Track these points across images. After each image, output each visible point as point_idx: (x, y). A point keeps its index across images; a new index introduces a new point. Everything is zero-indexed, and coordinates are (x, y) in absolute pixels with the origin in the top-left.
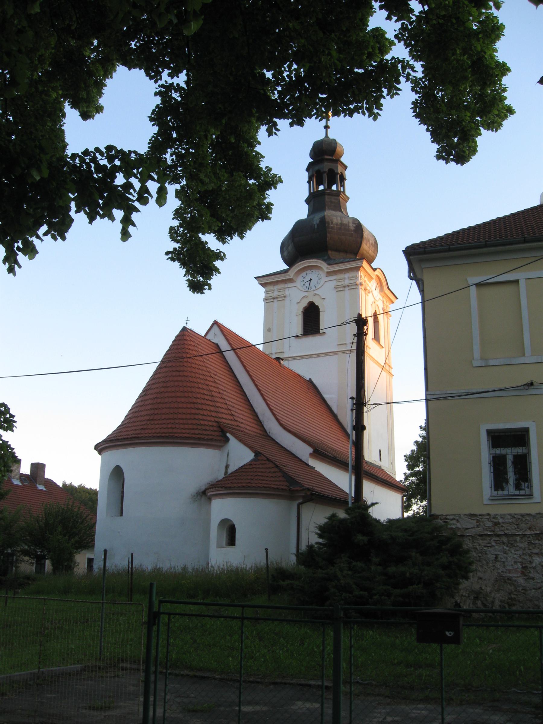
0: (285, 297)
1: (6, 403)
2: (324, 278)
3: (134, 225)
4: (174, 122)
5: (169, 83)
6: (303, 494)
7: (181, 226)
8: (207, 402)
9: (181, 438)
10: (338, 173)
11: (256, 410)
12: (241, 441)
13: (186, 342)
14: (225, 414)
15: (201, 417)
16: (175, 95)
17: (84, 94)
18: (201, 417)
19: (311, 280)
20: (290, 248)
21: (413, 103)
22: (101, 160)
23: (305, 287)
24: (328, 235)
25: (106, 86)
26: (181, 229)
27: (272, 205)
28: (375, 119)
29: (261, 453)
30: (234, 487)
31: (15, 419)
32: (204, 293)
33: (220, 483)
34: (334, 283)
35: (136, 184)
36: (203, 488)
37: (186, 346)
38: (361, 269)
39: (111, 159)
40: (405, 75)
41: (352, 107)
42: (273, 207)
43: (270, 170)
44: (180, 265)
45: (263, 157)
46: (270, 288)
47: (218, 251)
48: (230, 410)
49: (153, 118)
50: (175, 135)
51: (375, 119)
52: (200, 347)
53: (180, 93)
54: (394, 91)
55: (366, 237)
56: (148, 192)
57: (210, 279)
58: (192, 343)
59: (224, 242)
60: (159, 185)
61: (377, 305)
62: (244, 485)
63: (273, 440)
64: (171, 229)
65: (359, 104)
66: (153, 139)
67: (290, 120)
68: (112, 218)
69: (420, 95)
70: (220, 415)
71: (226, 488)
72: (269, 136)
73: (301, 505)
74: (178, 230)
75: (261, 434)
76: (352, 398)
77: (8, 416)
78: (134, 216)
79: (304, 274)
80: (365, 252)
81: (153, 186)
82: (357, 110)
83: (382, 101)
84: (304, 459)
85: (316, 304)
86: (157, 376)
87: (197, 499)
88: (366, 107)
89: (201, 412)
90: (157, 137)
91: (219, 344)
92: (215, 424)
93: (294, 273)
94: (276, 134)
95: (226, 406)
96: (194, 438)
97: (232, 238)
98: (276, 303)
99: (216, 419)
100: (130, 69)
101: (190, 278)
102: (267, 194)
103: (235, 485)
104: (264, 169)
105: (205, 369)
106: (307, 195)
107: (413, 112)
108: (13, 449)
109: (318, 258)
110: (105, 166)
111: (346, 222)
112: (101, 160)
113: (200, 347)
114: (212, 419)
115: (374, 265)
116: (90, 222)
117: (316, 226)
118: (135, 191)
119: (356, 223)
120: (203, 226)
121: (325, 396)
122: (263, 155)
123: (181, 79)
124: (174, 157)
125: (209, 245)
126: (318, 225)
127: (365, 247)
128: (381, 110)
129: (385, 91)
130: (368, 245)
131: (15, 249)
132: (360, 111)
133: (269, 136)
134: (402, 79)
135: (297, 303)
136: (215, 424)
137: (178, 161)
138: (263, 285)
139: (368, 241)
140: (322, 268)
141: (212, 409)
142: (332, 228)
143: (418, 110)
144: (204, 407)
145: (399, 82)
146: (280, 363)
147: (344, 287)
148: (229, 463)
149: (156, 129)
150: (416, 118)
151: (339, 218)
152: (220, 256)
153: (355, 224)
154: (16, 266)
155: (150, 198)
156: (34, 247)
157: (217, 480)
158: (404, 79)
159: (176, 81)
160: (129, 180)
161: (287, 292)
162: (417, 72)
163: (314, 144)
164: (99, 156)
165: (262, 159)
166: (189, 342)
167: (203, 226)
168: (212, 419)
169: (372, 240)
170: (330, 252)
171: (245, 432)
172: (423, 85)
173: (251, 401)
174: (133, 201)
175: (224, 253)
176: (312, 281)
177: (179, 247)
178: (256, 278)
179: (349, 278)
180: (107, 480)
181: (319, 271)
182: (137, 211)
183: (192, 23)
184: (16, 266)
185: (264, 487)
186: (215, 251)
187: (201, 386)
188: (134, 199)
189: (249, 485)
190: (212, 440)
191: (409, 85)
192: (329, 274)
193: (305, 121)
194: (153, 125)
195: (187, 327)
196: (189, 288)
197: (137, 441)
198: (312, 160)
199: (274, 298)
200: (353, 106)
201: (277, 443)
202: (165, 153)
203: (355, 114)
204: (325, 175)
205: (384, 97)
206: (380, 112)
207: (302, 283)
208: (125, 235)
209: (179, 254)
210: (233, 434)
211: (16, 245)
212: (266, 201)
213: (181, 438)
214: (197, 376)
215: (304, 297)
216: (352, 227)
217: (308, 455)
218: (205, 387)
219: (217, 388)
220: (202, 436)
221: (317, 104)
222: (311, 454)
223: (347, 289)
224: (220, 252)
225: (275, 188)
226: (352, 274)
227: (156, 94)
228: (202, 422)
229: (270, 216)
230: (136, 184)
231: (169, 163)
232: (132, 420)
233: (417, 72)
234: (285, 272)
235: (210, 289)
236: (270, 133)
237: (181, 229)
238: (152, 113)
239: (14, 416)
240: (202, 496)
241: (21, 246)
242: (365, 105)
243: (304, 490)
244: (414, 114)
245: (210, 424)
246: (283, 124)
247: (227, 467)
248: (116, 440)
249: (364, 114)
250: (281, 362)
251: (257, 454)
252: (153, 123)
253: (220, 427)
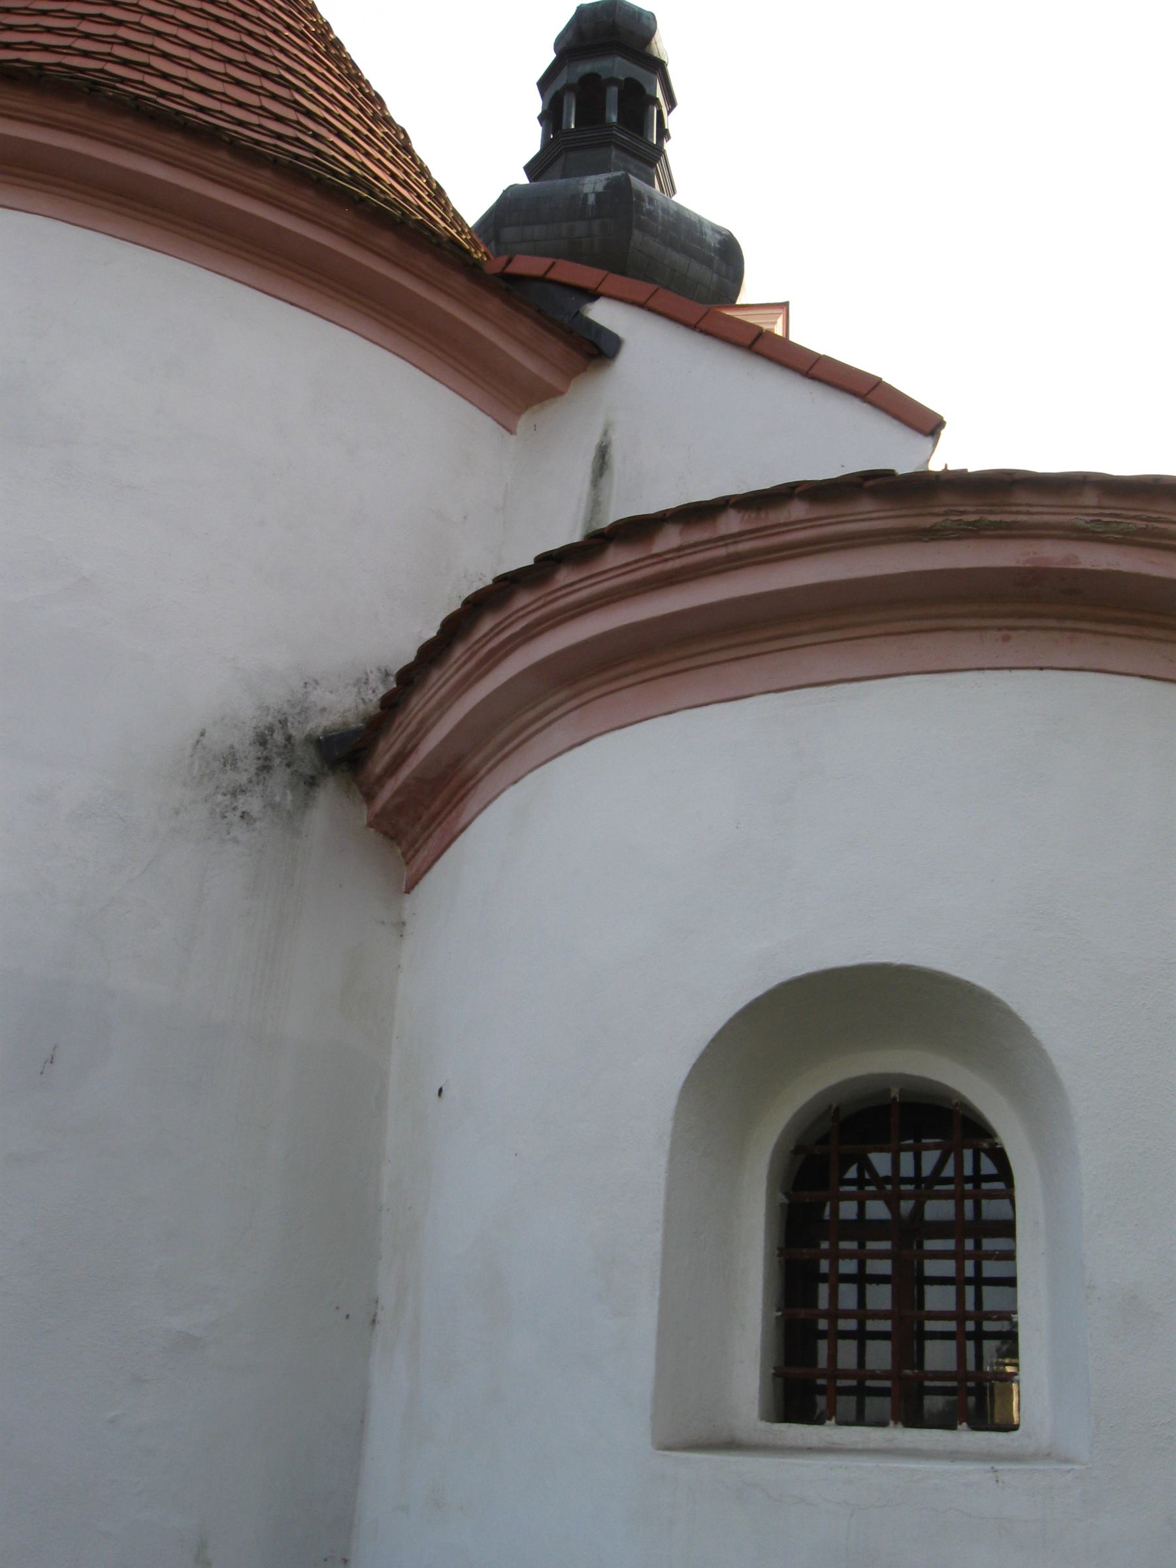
24: (637, 234)
87: (253, 804)
117: (591, 199)
126: (598, 195)
142: (650, 214)
163: (578, 8)
204: (613, 92)
240: (312, 782)
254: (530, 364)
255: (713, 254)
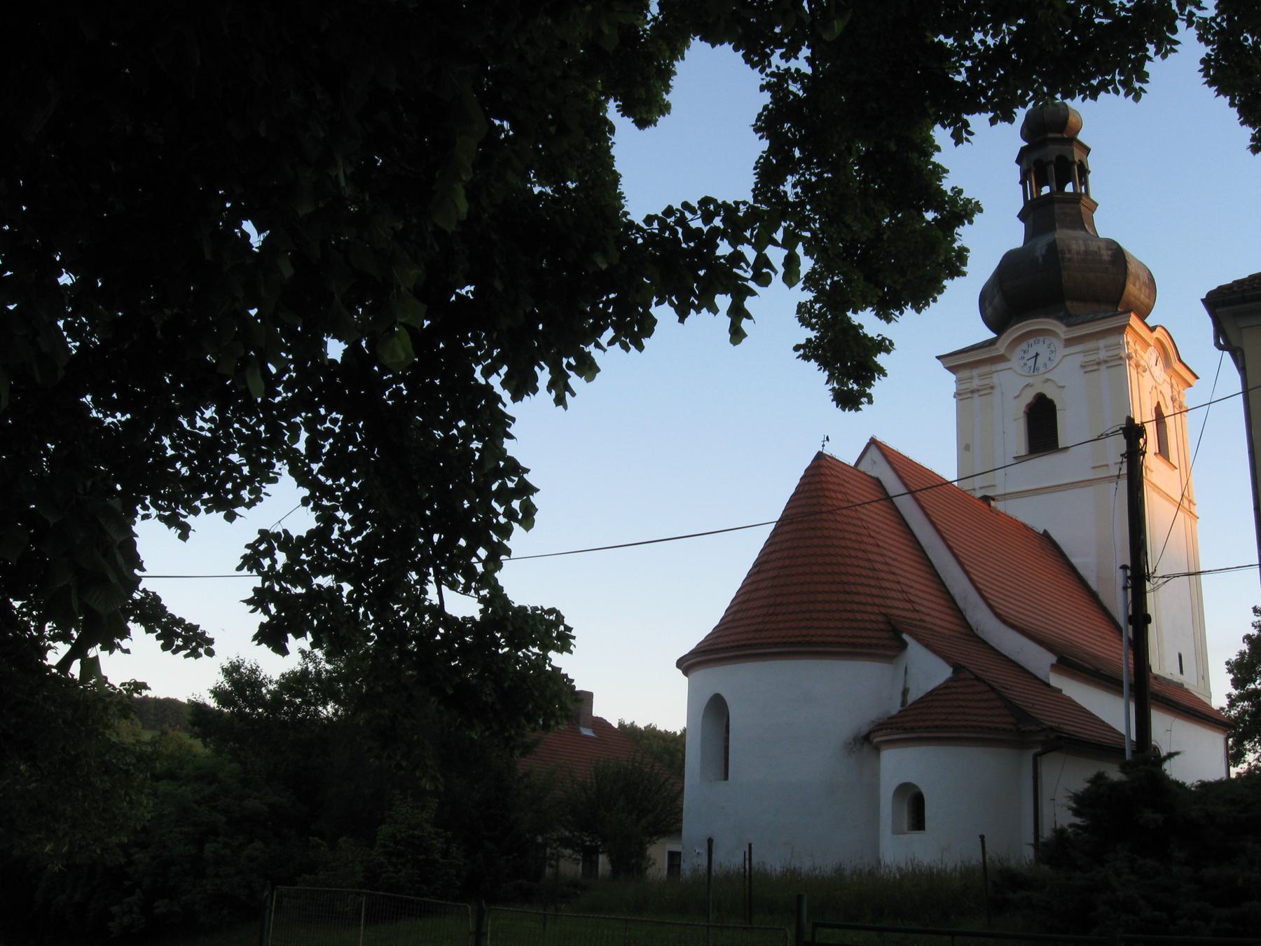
0: (992, 388)
1: (558, 609)
2: (1061, 351)
3: (749, 317)
4: (795, 132)
5: (782, 68)
6: (1043, 738)
7: (816, 300)
8: (864, 581)
9: (824, 644)
10: (1074, 162)
11: (952, 592)
12: (927, 646)
13: (823, 478)
14: (899, 600)
15: (855, 607)
16: (794, 88)
17: (642, 93)
18: (855, 607)
19: (1037, 355)
20: (997, 300)
21: (1203, 61)
22: (692, 220)
23: (1026, 368)
25: (675, 73)
26: (817, 306)
27: (967, 250)
28: (1137, 98)
29: (964, 667)
30: (920, 728)
31: (573, 633)
32: (861, 409)
33: (894, 720)
34: (1080, 359)
35: (750, 253)
36: (865, 730)
37: (825, 486)
38: (1128, 329)
39: (707, 218)
40: (1185, 18)
41: (1095, 82)
42: (968, 254)
43: (960, 192)
44: (818, 365)
45: (946, 171)
46: (965, 373)
47: (880, 338)
48: (906, 593)
49: (760, 126)
50: (797, 154)
51: (1137, 98)
52: (848, 485)
53: (802, 83)
54: (1166, 46)
55: (1133, 270)
56: (768, 264)
57: (870, 386)
58: (836, 480)
59: (888, 319)
60: (785, 252)
61: (1161, 392)
62: (936, 723)
63: (985, 642)
64: (801, 306)
65: (1107, 77)
66: (762, 160)
67: (991, 115)
68: (714, 310)
69: (1215, 47)
70: (889, 602)
71: (905, 730)
72: (956, 144)
73: (1038, 758)
74: (812, 307)
75: (962, 634)
76: (1124, 567)
77: (562, 628)
78: (749, 303)
79: (1024, 346)
80: (1132, 299)
81: (776, 255)
82: (1103, 87)
83: (1148, 67)
84: (1041, 675)
85: (1049, 396)
86: (777, 539)
88: (1120, 81)
89: (856, 598)
90: (768, 157)
91: (881, 478)
92: (880, 618)
93: (1006, 344)
94: (968, 140)
95: (898, 587)
96: (847, 644)
97: (902, 313)
98: (977, 400)
99: (883, 610)
100: (713, 46)
101: (835, 385)
102: (956, 234)
103: (921, 724)
104: (949, 193)
105: (859, 523)
106: (1020, 205)
107: (1204, 76)
108: (573, 681)
109: (1047, 315)
110: (699, 230)
111: (1096, 249)
112: (692, 220)
113: (848, 485)
114: (876, 609)
115: (1150, 320)
116: (682, 320)
117: (1041, 259)
118: (748, 265)
119: (1114, 247)
120: (854, 299)
121: (1075, 561)
122: (946, 167)
123: (800, 63)
124: (799, 190)
125: (866, 330)
127: (1133, 289)
128: (1147, 82)
129: (1151, 49)
130: (1138, 286)
131: (564, 366)
132: (1110, 88)
133: (956, 144)
134: (1181, 25)
135: (1016, 397)
136: (880, 618)
137: (806, 195)
138: (952, 369)
139: (1137, 277)
140: (1057, 334)
141: (874, 591)
142: (1070, 260)
143: (1212, 73)
144: (860, 589)
145: (1174, 30)
146: (989, 505)
147: (1098, 364)
148: (907, 686)
149: (765, 144)
150: (1210, 86)
151: (1081, 242)
152: (883, 346)
153: (1111, 249)
154: (567, 394)
155: (773, 274)
156: (592, 360)
157: (888, 716)
158: (1185, 24)
159: (793, 64)
160: (738, 248)
161: (995, 379)
162: (1206, 9)
164: (688, 215)
165: (945, 175)
166: (829, 479)
167: (854, 299)
168: (876, 609)
169: (1144, 278)
170: (1068, 304)
171: (935, 631)
172: (1217, 29)
173: (942, 575)
174: (747, 280)
175: (890, 342)
176: (1038, 357)
177: (815, 337)
178: (938, 358)
179: (1106, 347)
180: (700, 718)
181: (1050, 338)
182: (753, 293)
183: (835, 22)
184: (567, 394)
185: (972, 726)
186: (876, 338)
187: (853, 553)
188: (749, 277)
189: (944, 723)
190: (877, 646)
191: (1193, 32)
192: (1069, 342)
193: (1015, 113)
194: (761, 138)
195: (824, 452)
196: (835, 403)
197: (748, 652)
198: (1027, 144)
199: (972, 392)
200: (1097, 80)
201: (993, 648)
202: (782, 181)
203: (1102, 95)
204: (1052, 169)
205: (1150, 59)
206: (1144, 86)
207: (1022, 362)
208: (737, 335)
209: (816, 348)
210: (911, 634)
211: (565, 361)
212: (955, 245)
213: (824, 644)
214: (847, 535)
215: (1028, 385)
216: (1106, 255)
217: (1048, 668)
218: (860, 554)
219: (881, 555)
220: (861, 641)
221: (1035, 81)
222: (1053, 665)
223: (1103, 367)
224: (884, 339)
225: (971, 222)
226: (1111, 340)
227: (762, 88)
228: (858, 616)
229: (965, 269)
230: (750, 253)
231: (791, 198)
232: (739, 615)
233: (1206, 9)
234: (989, 344)
235: (870, 402)
236: (958, 140)
237: (817, 306)
238: (758, 119)
239: (572, 628)
240: (863, 744)
241: (574, 363)
242: (1117, 78)
243: (1043, 730)
244: (1206, 79)
245: (873, 618)
246: (978, 121)
247: (905, 692)
248: (712, 650)
249: (1117, 92)
250: (993, 503)
251: (957, 668)
252: (759, 135)
253: (889, 623)
254: (890, 653)
255: (1108, 266)
